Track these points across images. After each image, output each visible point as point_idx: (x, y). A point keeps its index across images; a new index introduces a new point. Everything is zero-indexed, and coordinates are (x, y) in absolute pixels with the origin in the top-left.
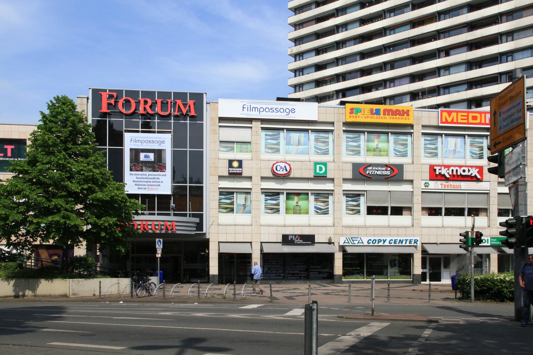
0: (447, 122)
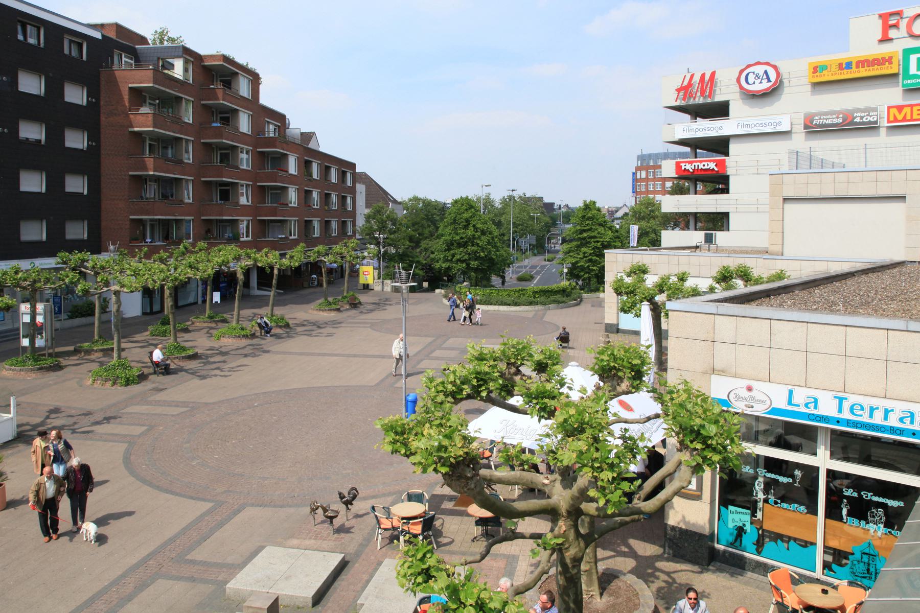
0: (896, 120)
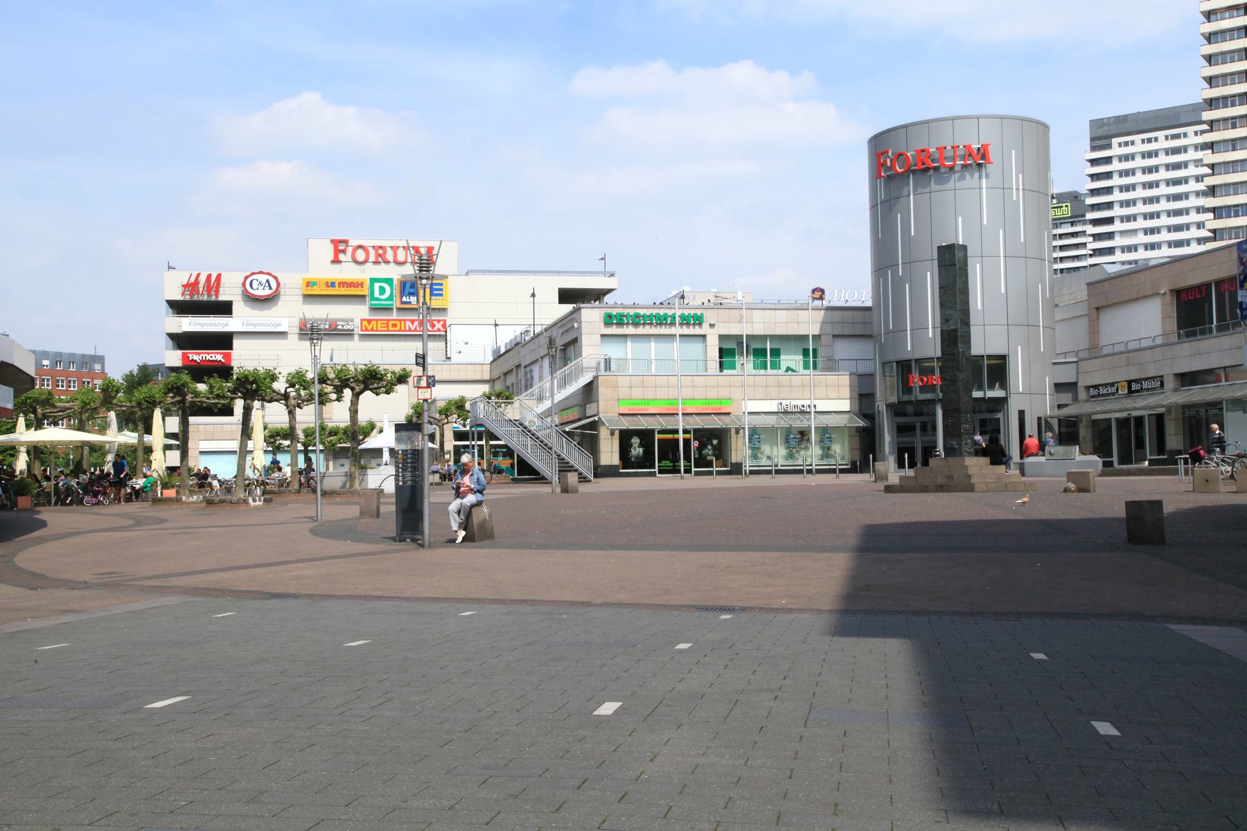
0: (367, 330)
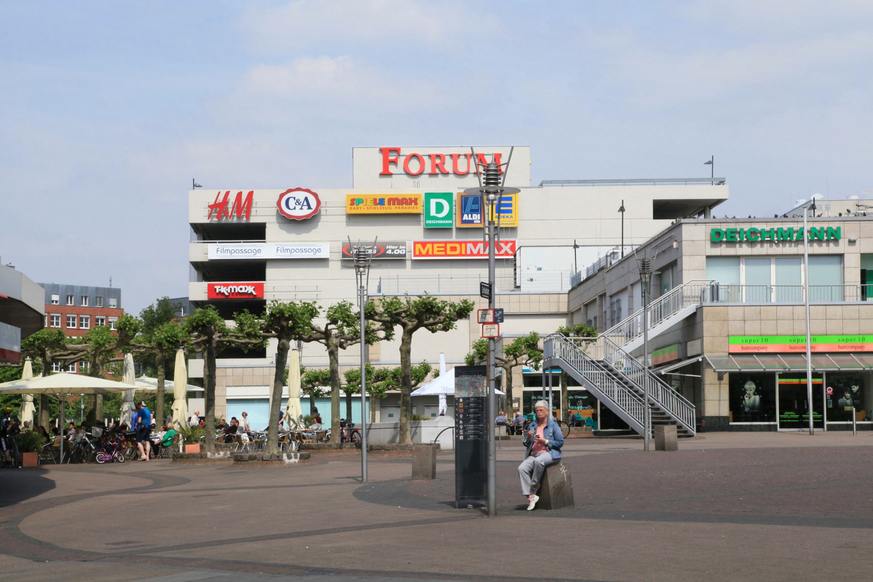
0: (421, 255)
